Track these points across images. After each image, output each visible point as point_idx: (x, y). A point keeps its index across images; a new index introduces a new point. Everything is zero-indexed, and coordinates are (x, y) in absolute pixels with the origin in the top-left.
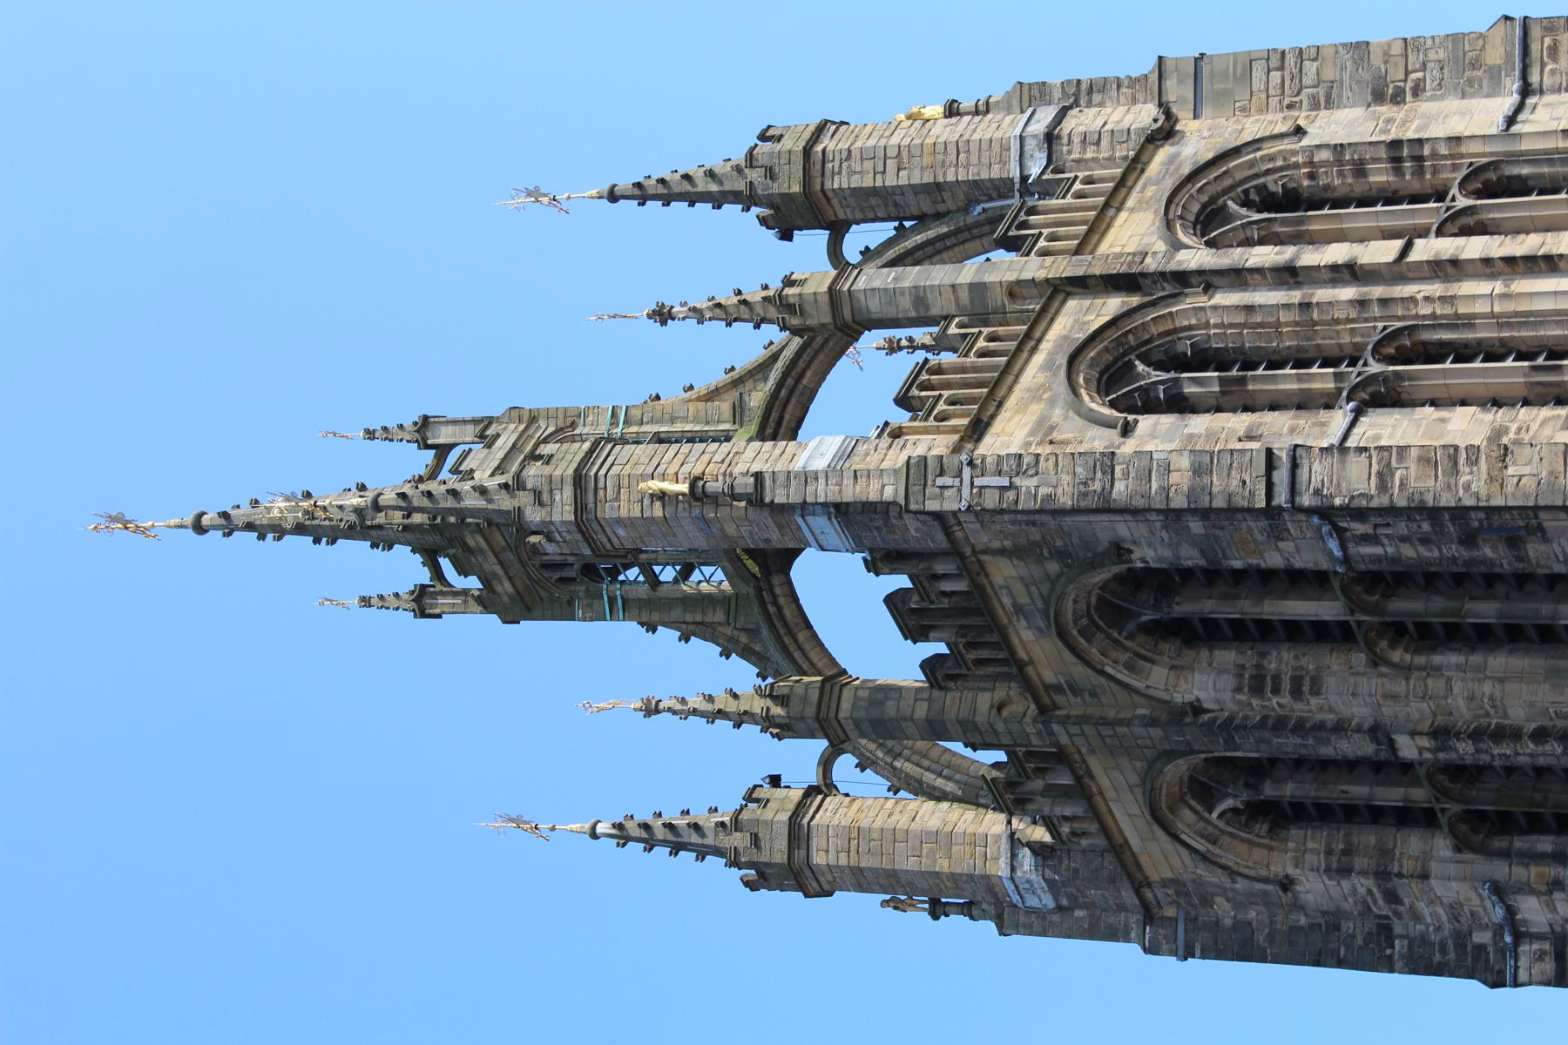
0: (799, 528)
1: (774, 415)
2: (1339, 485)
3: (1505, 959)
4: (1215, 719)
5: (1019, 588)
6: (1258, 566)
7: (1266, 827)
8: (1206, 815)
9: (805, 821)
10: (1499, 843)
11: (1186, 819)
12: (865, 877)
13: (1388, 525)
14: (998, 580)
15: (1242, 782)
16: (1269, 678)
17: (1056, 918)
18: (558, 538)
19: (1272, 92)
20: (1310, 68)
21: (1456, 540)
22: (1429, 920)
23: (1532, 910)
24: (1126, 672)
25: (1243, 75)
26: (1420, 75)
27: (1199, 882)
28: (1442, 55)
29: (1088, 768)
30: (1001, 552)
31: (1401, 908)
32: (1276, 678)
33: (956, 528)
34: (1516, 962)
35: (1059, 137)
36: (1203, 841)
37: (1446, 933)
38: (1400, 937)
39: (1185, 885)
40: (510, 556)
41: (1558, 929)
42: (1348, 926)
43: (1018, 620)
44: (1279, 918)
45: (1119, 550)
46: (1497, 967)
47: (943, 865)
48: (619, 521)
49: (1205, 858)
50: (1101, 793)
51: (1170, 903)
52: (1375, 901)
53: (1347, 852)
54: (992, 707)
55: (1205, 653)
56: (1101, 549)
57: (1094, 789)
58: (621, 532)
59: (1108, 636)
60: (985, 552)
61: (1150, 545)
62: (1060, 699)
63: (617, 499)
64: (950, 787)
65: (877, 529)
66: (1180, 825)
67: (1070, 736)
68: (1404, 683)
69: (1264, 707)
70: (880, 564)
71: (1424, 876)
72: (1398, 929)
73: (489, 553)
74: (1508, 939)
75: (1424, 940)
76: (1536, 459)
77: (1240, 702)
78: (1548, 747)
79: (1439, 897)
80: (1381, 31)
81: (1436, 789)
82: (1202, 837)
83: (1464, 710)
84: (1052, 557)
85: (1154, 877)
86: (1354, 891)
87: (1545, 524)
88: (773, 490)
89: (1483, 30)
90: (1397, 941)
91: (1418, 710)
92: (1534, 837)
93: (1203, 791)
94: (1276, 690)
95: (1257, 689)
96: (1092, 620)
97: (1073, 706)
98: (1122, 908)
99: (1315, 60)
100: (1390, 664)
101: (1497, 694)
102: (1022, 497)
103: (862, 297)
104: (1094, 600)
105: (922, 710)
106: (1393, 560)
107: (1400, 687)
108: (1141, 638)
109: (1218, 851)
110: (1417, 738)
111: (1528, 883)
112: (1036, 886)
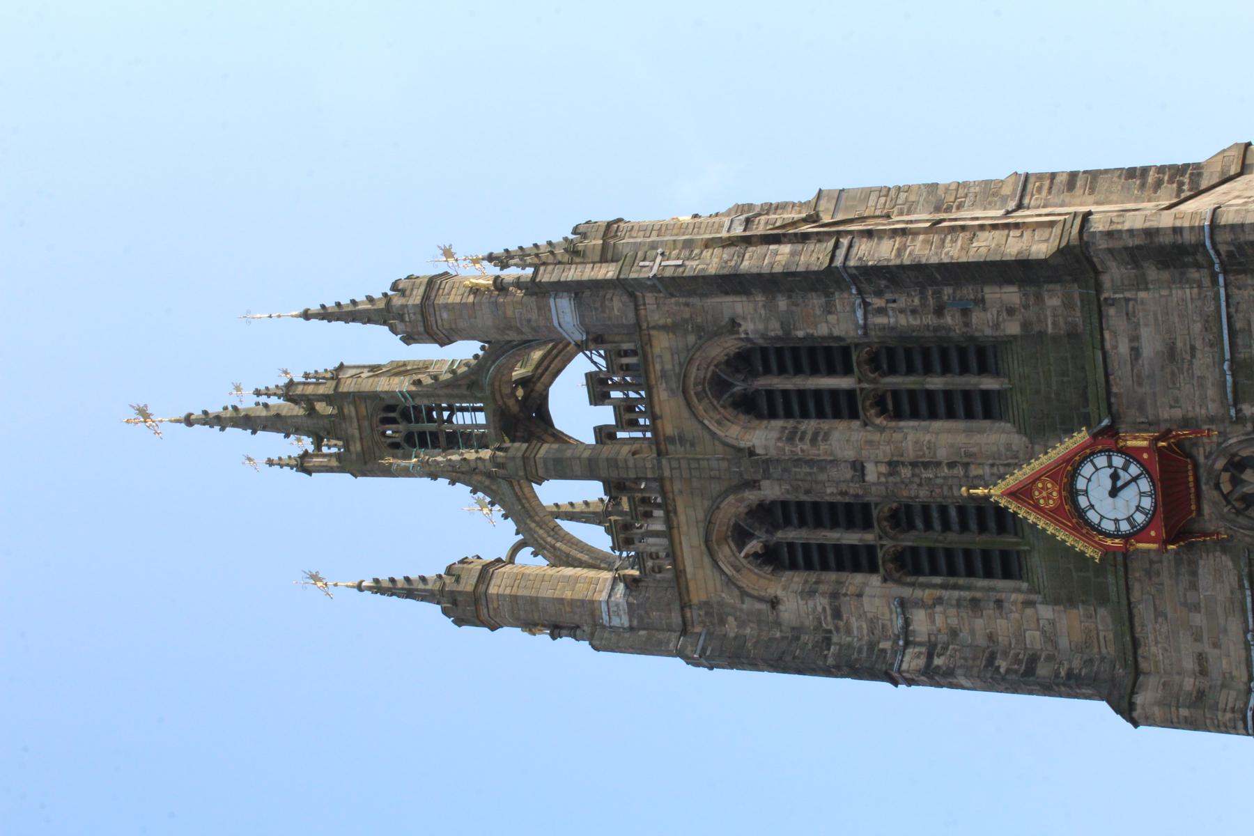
0: (550, 310)
1: (546, 363)
2: (873, 255)
3: (896, 656)
4: (758, 459)
5: (667, 357)
6: (812, 335)
7: (771, 569)
8: (737, 554)
9: (491, 570)
10: (910, 579)
11: (725, 552)
12: (517, 604)
13: (894, 301)
14: (657, 351)
15: (764, 529)
16: (799, 433)
17: (627, 635)
18: (407, 319)
19: (878, 207)
20: (903, 196)
21: (932, 310)
22: (855, 633)
23: (921, 622)
24: (716, 425)
25: (865, 198)
26: (963, 199)
27: (721, 604)
28: (977, 189)
29: (675, 506)
30: (664, 328)
31: (841, 624)
32: (804, 433)
33: (642, 307)
34: (903, 657)
35: (753, 221)
36: (731, 568)
37: (864, 643)
38: (835, 644)
39: (712, 607)
40: (366, 423)
41: (933, 638)
42: (805, 638)
43: (661, 384)
44: (764, 633)
45: (734, 325)
46: (890, 661)
47: (568, 595)
48: (446, 306)
49: (730, 581)
50: (678, 527)
51: (700, 622)
52: (825, 618)
53: (817, 583)
54: (629, 452)
55: (765, 422)
56: (723, 324)
57: (675, 523)
58: (445, 316)
59: (711, 403)
60: (654, 328)
61: (753, 320)
62: (671, 448)
63: (449, 294)
64: (585, 557)
65: (596, 309)
66: (720, 555)
67: (671, 469)
68: (879, 435)
69: (792, 451)
70: (590, 343)
71: (860, 595)
72: (835, 639)
73: (355, 420)
74: (901, 643)
75: (850, 646)
76: (991, 238)
77: (778, 447)
78: (955, 471)
79: (865, 613)
80: (946, 176)
81: (880, 528)
82: (732, 566)
83: (911, 452)
84: (693, 332)
85: (695, 600)
86: (815, 608)
87: (987, 296)
88: (543, 275)
89: (1003, 179)
90: (832, 648)
91: (884, 452)
92: (931, 577)
93: (741, 536)
94: (802, 439)
95: (791, 439)
96: (704, 389)
97: (677, 450)
98: (670, 629)
99: (906, 192)
100: (873, 425)
101: (933, 440)
102: (687, 270)
103: (620, 248)
104: (709, 374)
105: (587, 454)
106: (893, 329)
107: (876, 437)
108: (730, 410)
110: (879, 464)
111: (922, 600)
112: (621, 608)
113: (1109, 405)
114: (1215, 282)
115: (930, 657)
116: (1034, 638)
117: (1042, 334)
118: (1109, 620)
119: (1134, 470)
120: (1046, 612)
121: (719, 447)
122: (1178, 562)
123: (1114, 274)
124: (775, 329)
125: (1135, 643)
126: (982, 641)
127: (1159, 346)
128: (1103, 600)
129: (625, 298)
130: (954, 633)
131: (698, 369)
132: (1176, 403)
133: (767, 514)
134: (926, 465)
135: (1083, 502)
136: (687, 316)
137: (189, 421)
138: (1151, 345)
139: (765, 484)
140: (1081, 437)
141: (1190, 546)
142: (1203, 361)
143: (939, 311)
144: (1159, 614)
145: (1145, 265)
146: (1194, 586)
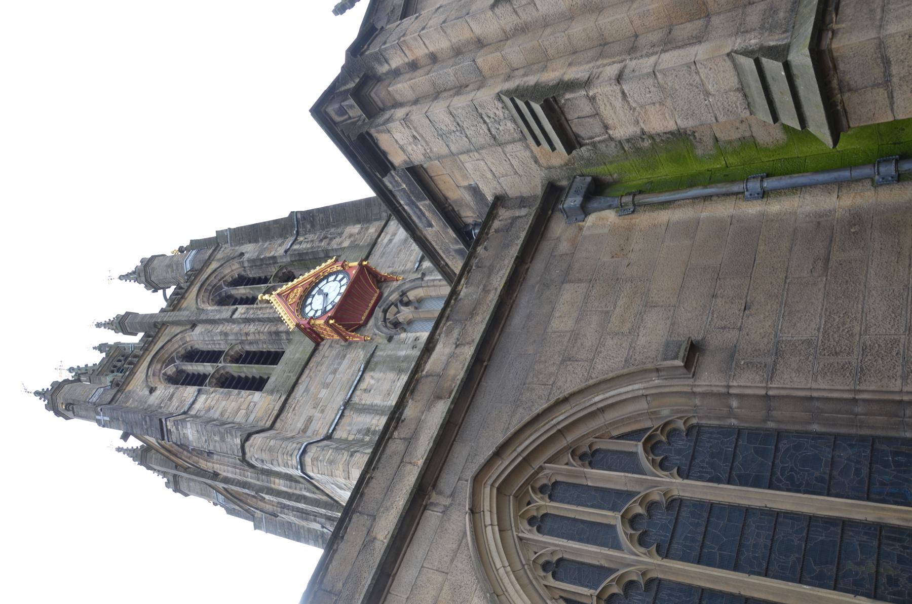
57: (151, 348)
109: (151, 377)
122: (337, 356)
131: (215, 277)
135: (309, 301)
143: (321, 241)
144: (307, 390)
146: (335, 372)
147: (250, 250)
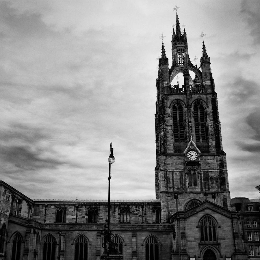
5: (203, 97)
14: (204, 96)
23: (169, 128)
27: (168, 100)
30: (207, 97)
45: (208, 107)
71: (172, 120)
85: (168, 96)
106: (209, 129)
113: (202, 156)
114: (218, 170)
115: (165, 129)
116: (168, 143)
117: (209, 148)
118: (172, 153)
119: (196, 158)
120: (172, 145)
121: (191, 103)
122: (182, 162)
123: (219, 158)
124: (208, 113)
125: (170, 156)
126: (167, 136)
127: (209, 162)
128: (175, 152)
129: (211, 92)
130: (168, 132)
132: (202, 164)
133: (181, 108)
134: (191, 131)
136: (209, 100)
137: (177, 16)
138: (210, 161)
139: (187, 109)
140: (200, 152)
141: (184, 164)
142: (209, 168)
143: (211, 135)
145: (220, 162)
146: (179, 164)
147: (210, 109)
